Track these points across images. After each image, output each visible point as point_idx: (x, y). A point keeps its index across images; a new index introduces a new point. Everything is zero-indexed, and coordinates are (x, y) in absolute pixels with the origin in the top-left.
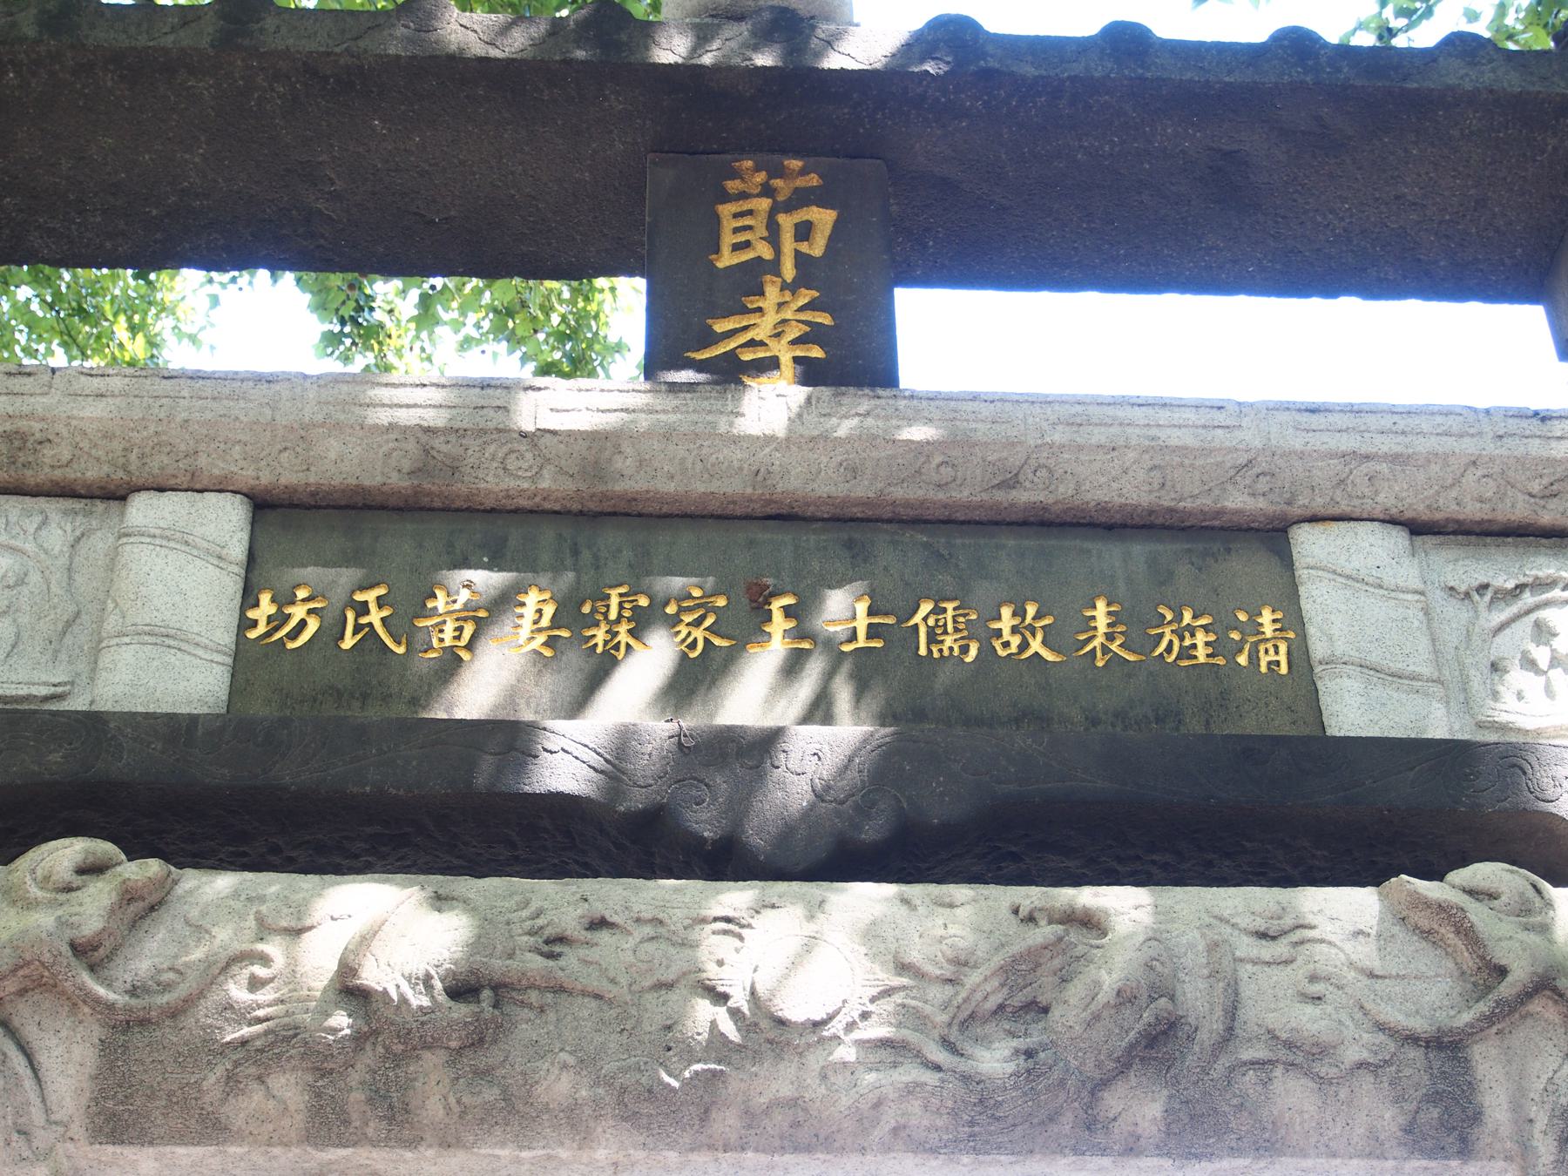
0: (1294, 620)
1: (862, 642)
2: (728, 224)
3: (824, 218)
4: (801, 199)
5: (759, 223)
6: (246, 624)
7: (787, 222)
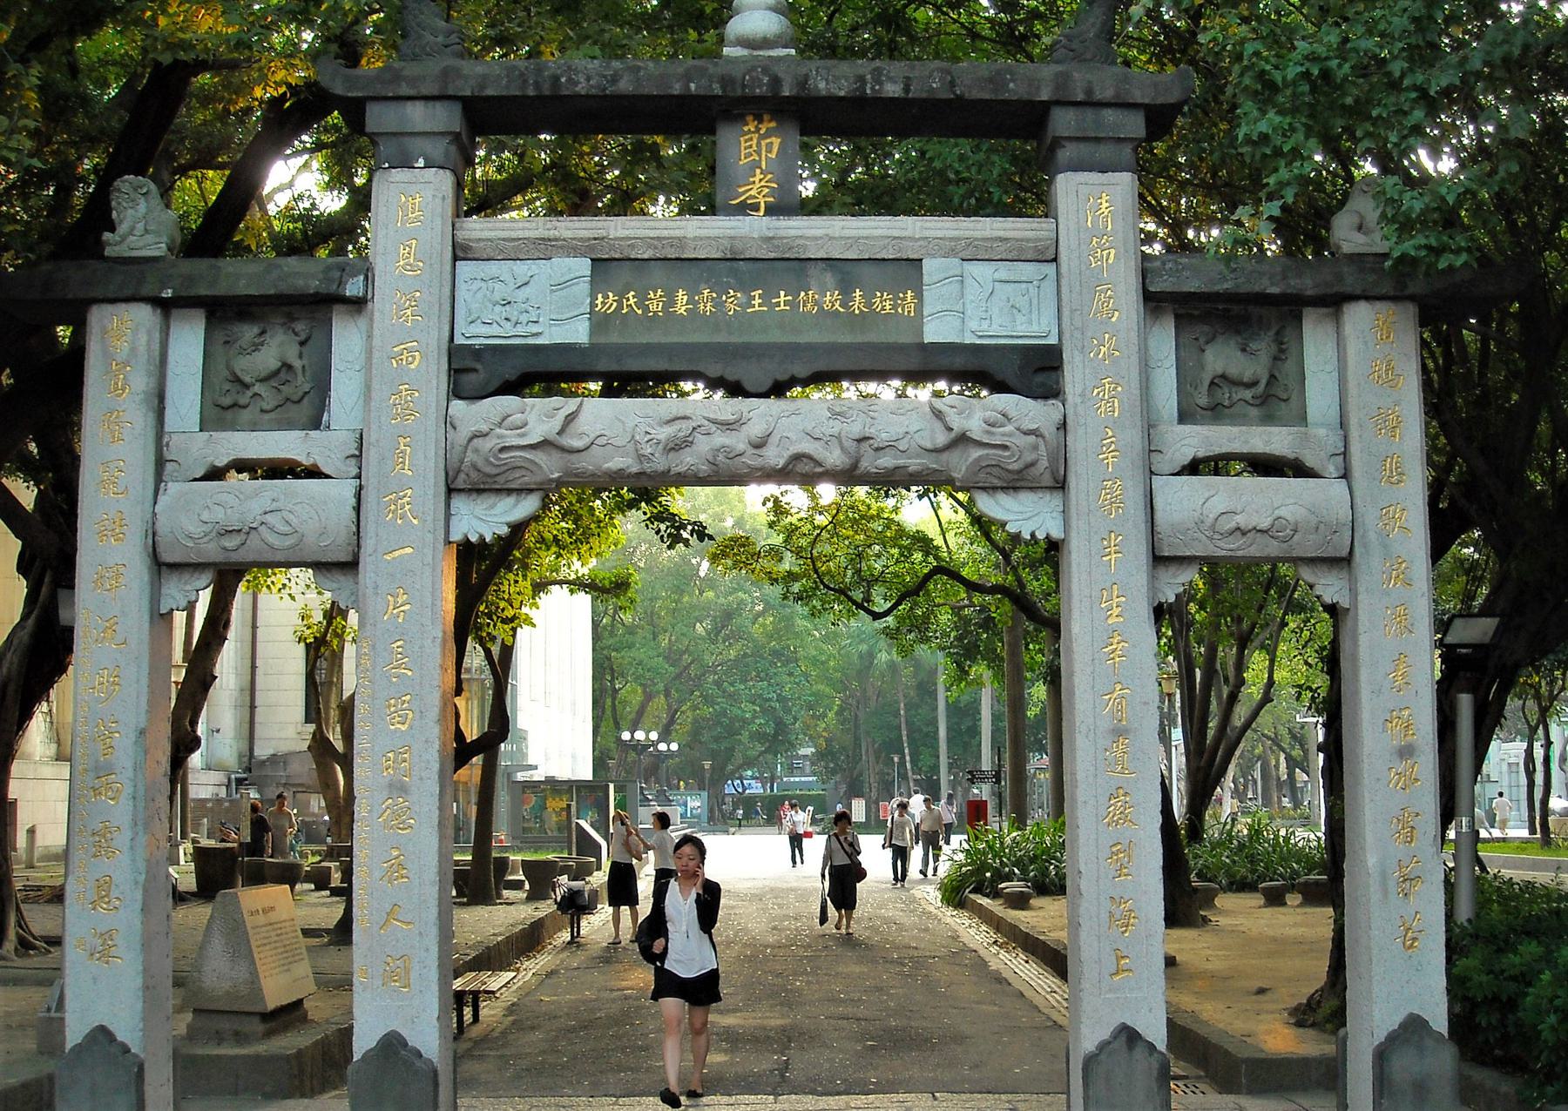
0: (919, 295)
1: (782, 307)
2: (743, 145)
3: (776, 141)
5: (755, 141)
6: (593, 305)
7: (763, 143)
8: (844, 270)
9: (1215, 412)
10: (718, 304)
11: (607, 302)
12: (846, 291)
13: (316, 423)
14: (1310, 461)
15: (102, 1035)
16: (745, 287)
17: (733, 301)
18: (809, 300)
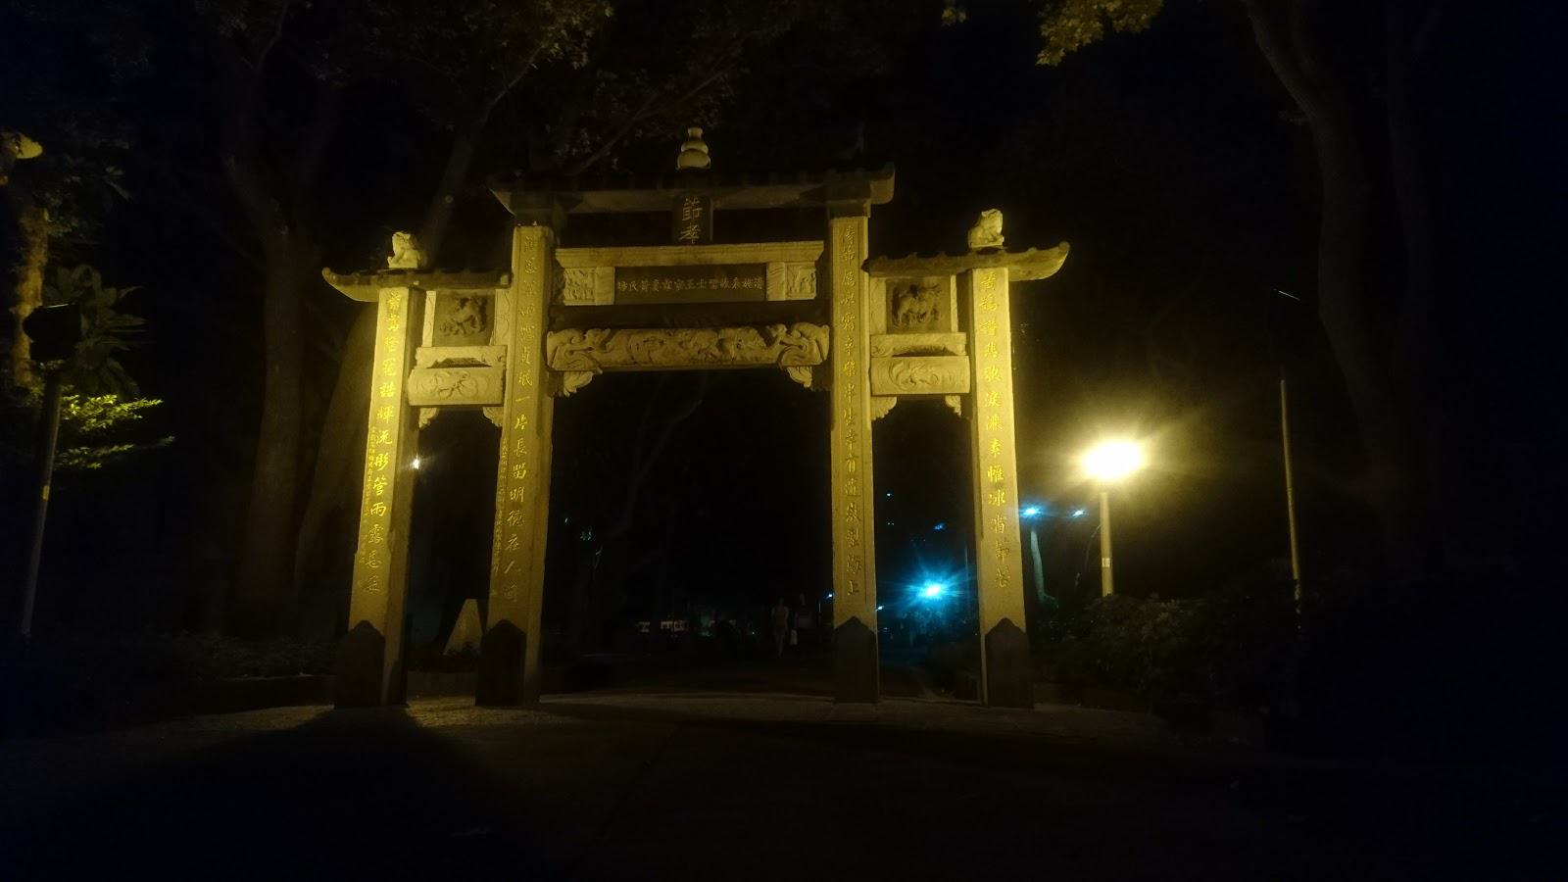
4: (697, 206)
8: (732, 271)
9: (906, 330)
10: (673, 286)
11: (623, 286)
12: (731, 281)
13: (486, 342)
14: (950, 348)
15: (365, 625)
17: (679, 285)
18: (714, 283)
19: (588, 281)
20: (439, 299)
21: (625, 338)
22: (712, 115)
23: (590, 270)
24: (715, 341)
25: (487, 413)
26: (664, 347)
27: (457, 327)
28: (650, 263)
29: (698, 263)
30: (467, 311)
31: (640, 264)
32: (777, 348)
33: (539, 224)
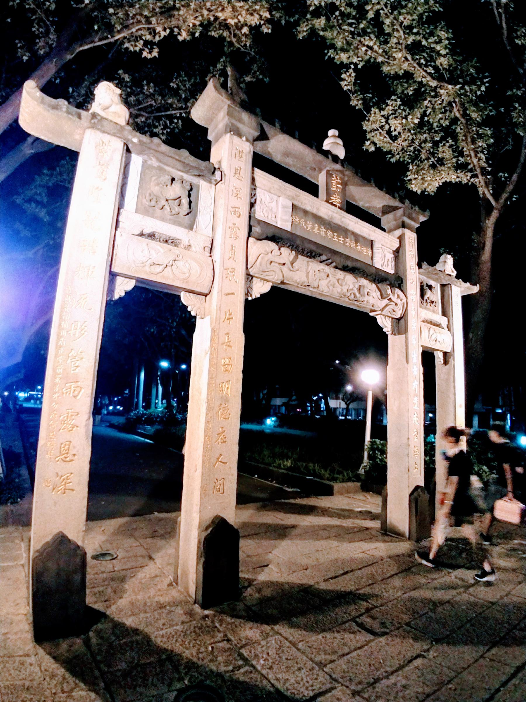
8: (357, 238)
16: (333, 231)
19: (274, 204)
20: (145, 166)
21: (305, 263)
22: (165, 132)
23: (275, 197)
24: (357, 286)
25: (185, 299)
26: (329, 279)
27: (164, 202)
28: (315, 211)
29: (340, 223)
30: (176, 190)
31: (308, 208)
32: (386, 301)
33: (247, 140)
